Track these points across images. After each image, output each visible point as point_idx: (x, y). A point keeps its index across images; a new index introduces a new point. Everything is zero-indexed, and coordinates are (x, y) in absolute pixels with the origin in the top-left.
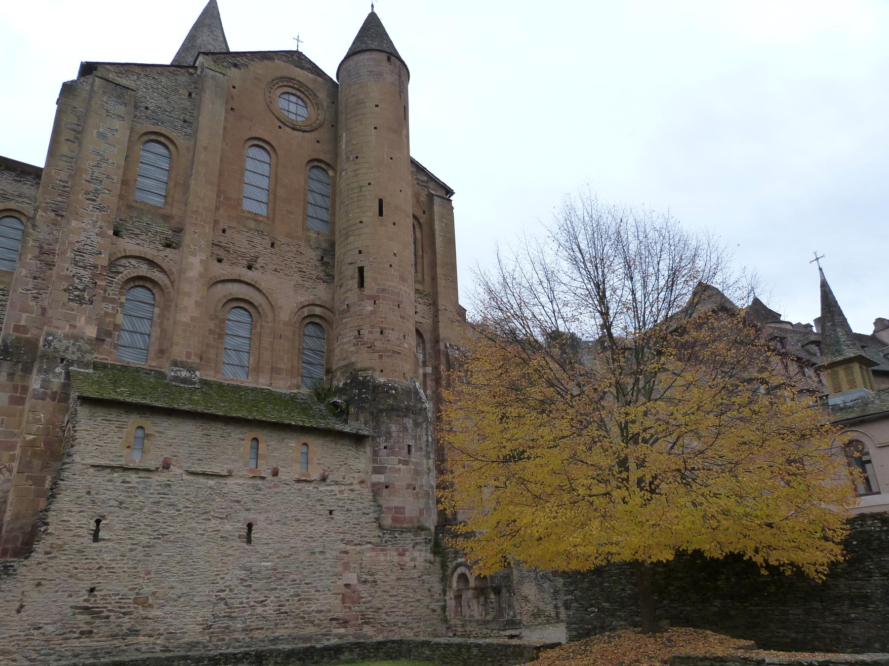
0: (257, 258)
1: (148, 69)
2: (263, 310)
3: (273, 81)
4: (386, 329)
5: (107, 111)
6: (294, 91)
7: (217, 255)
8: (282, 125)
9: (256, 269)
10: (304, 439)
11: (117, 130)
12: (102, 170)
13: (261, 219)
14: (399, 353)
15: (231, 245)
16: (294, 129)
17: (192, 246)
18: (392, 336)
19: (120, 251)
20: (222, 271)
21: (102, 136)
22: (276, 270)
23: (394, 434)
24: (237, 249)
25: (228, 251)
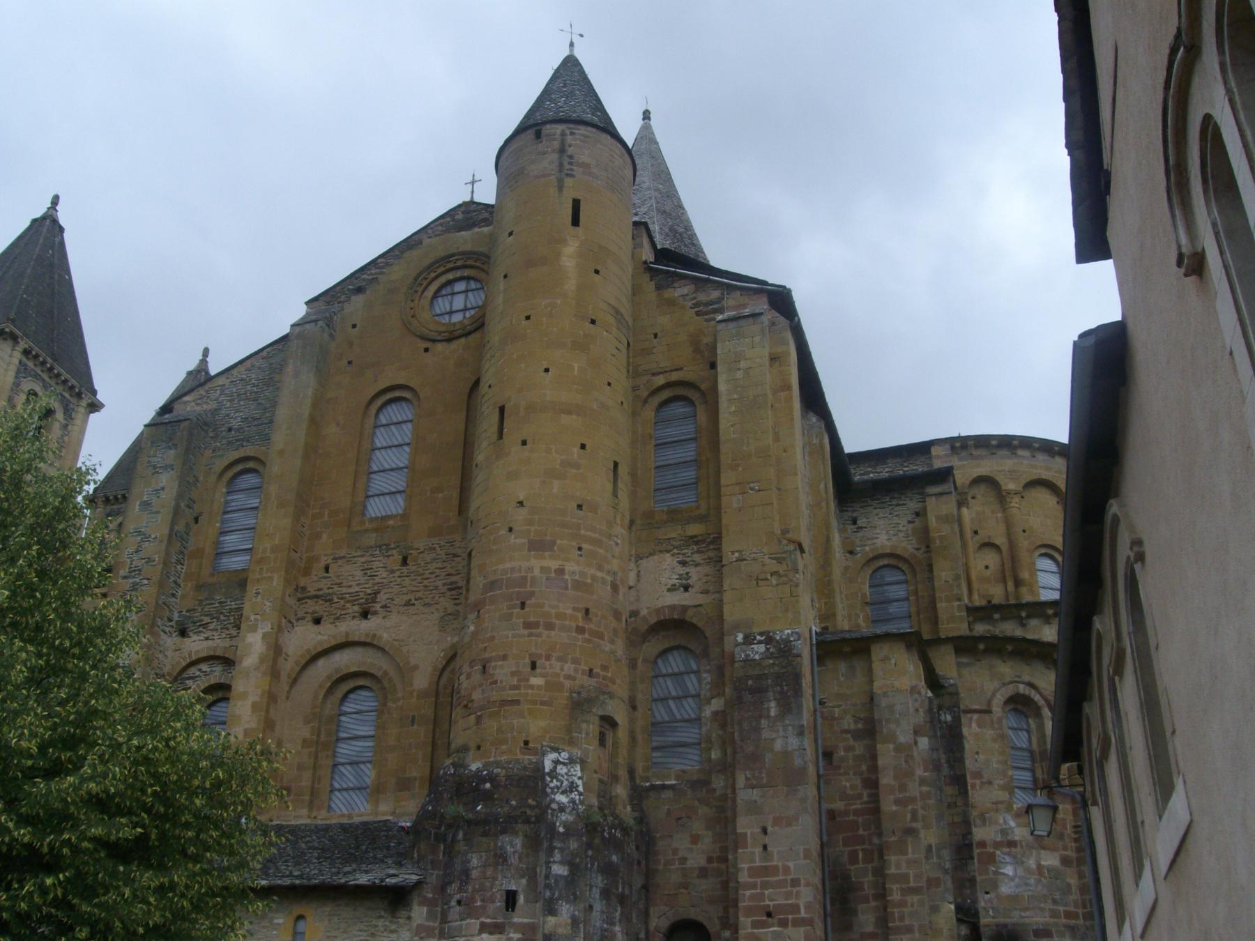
0: (376, 593)
1: (235, 372)
2: (390, 680)
3: (416, 279)
4: (489, 660)
5: (155, 467)
6: (458, 274)
7: (314, 612)
8: (428, 345)
9: (375, 613)
10: (298, 910)
11: (163, 489)
12: (142, 555)
13: (391, 522)
14: (517, 702)
15: (336, 588)
16: (449, 340)
17: (252, 618)
18: (502, 671)
19: (184, 659)
20: (320, 637)
21: (146, 505)
22: (408, 603)
23: (474, 874)
24: (344, 590)
25: (330, 601)
